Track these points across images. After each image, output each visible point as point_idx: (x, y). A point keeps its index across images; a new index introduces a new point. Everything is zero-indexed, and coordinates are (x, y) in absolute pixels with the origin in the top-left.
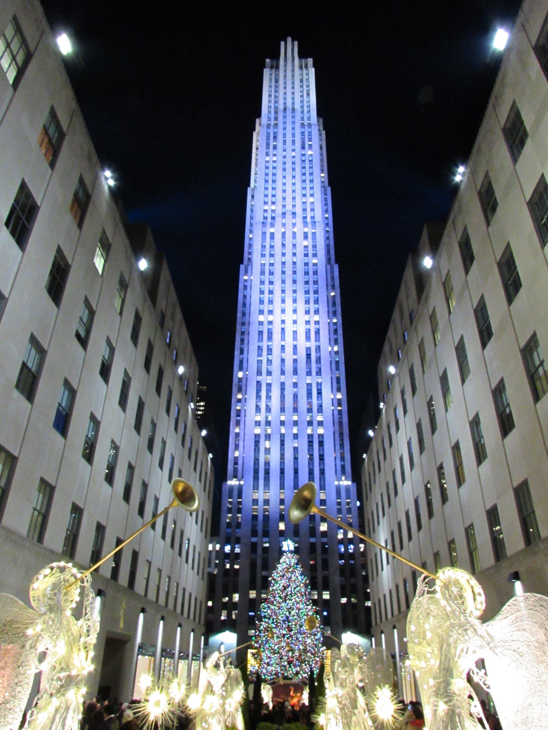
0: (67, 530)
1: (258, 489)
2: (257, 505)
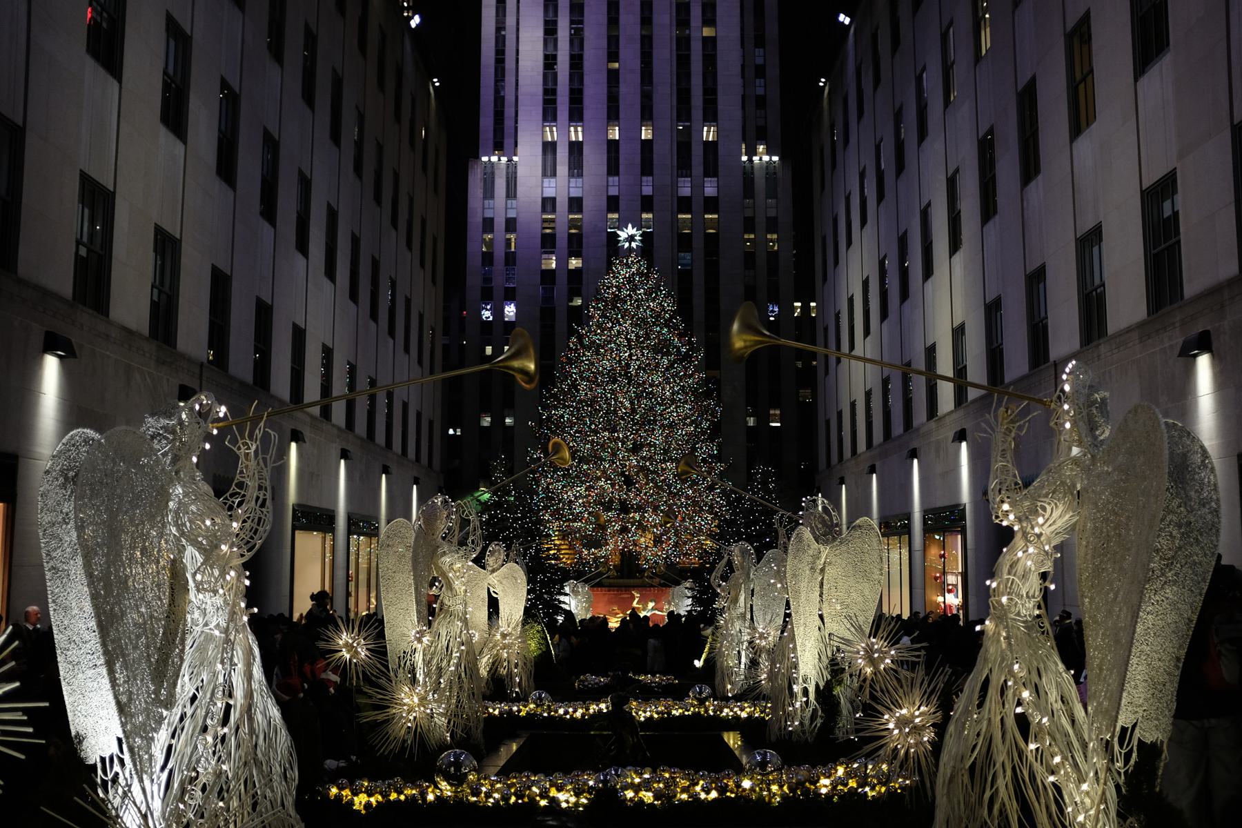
0: (79, 243)
1: (554, 174)
2: (554, 211)
